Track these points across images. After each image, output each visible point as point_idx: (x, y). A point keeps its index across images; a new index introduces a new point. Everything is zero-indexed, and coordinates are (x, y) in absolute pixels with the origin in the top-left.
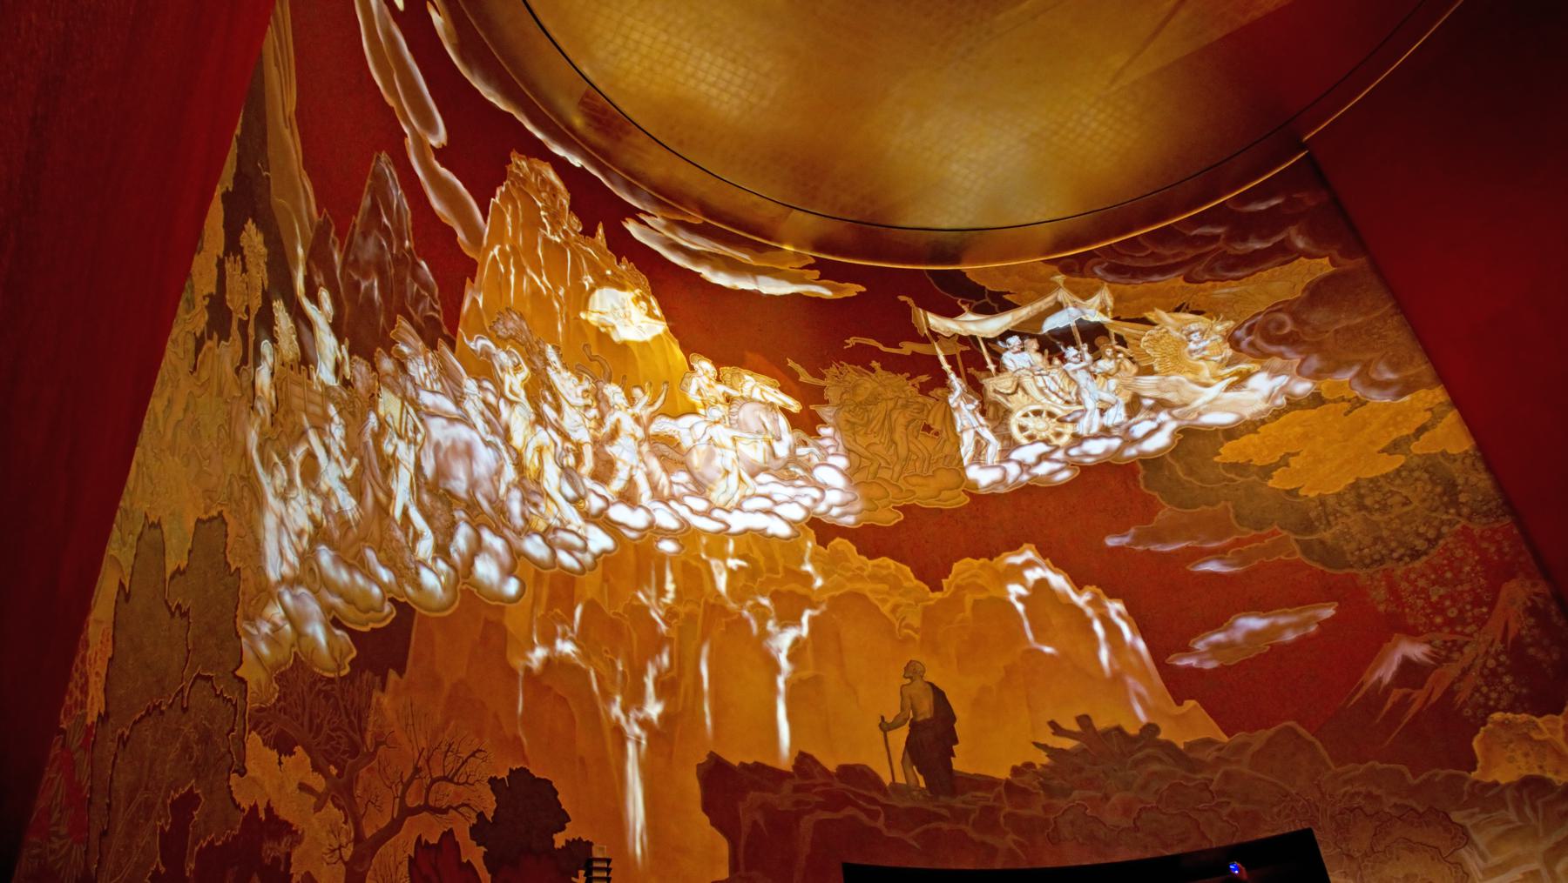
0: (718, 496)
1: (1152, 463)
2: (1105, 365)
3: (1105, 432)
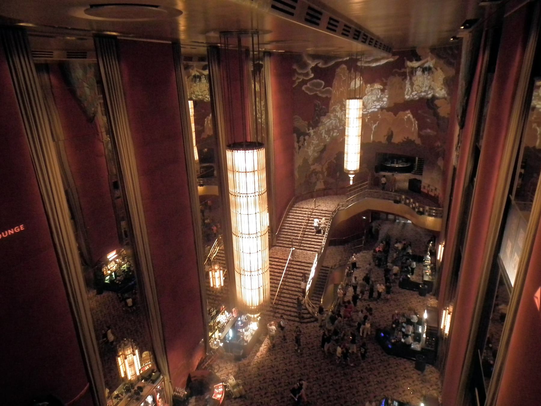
0: (368, 108)
1: (428, 100)
2: (429, 77)
3: (425, 91)
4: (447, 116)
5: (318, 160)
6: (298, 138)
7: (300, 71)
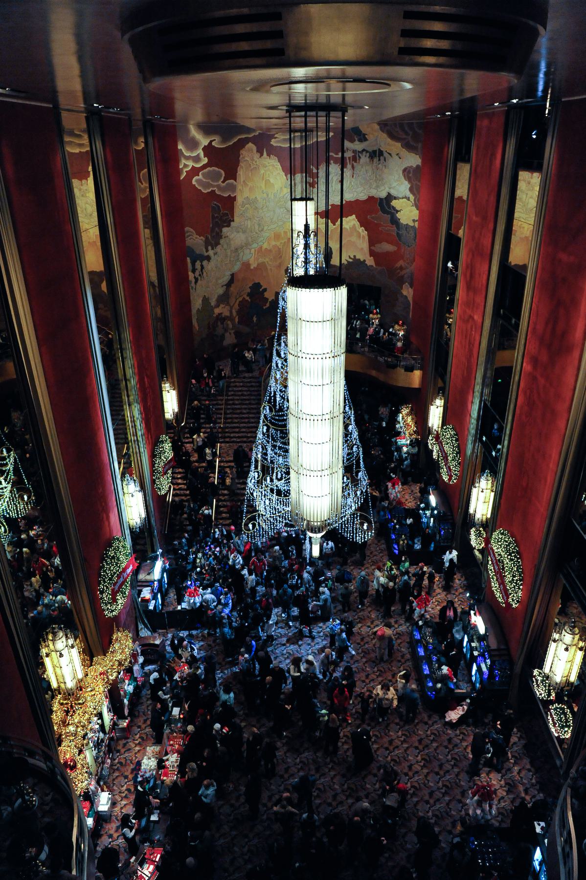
4: (411, 224)
5: (224, 299)
7: (187, 154)
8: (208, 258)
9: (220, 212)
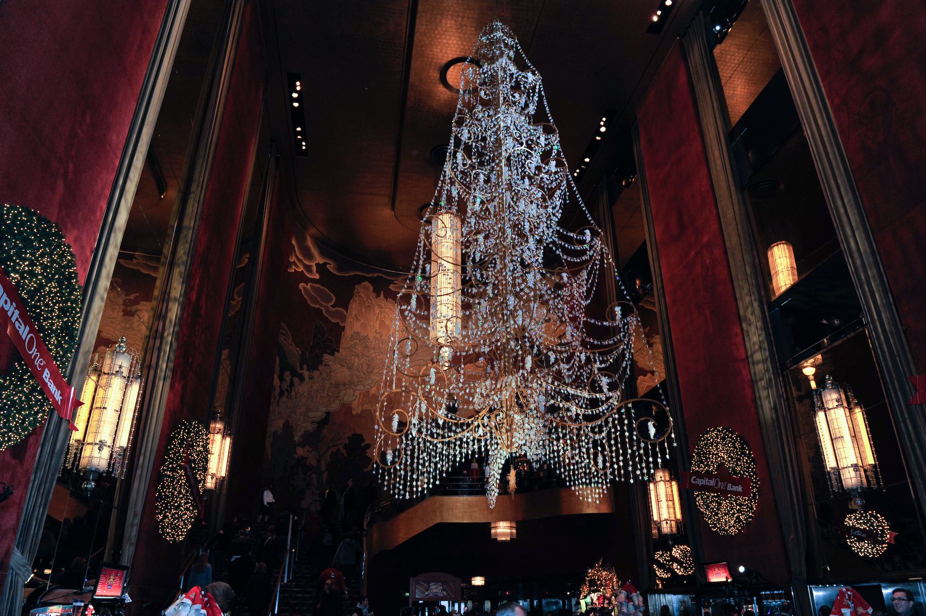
6: (283, 369)
8: (302, 378)
9: (325, 339)
